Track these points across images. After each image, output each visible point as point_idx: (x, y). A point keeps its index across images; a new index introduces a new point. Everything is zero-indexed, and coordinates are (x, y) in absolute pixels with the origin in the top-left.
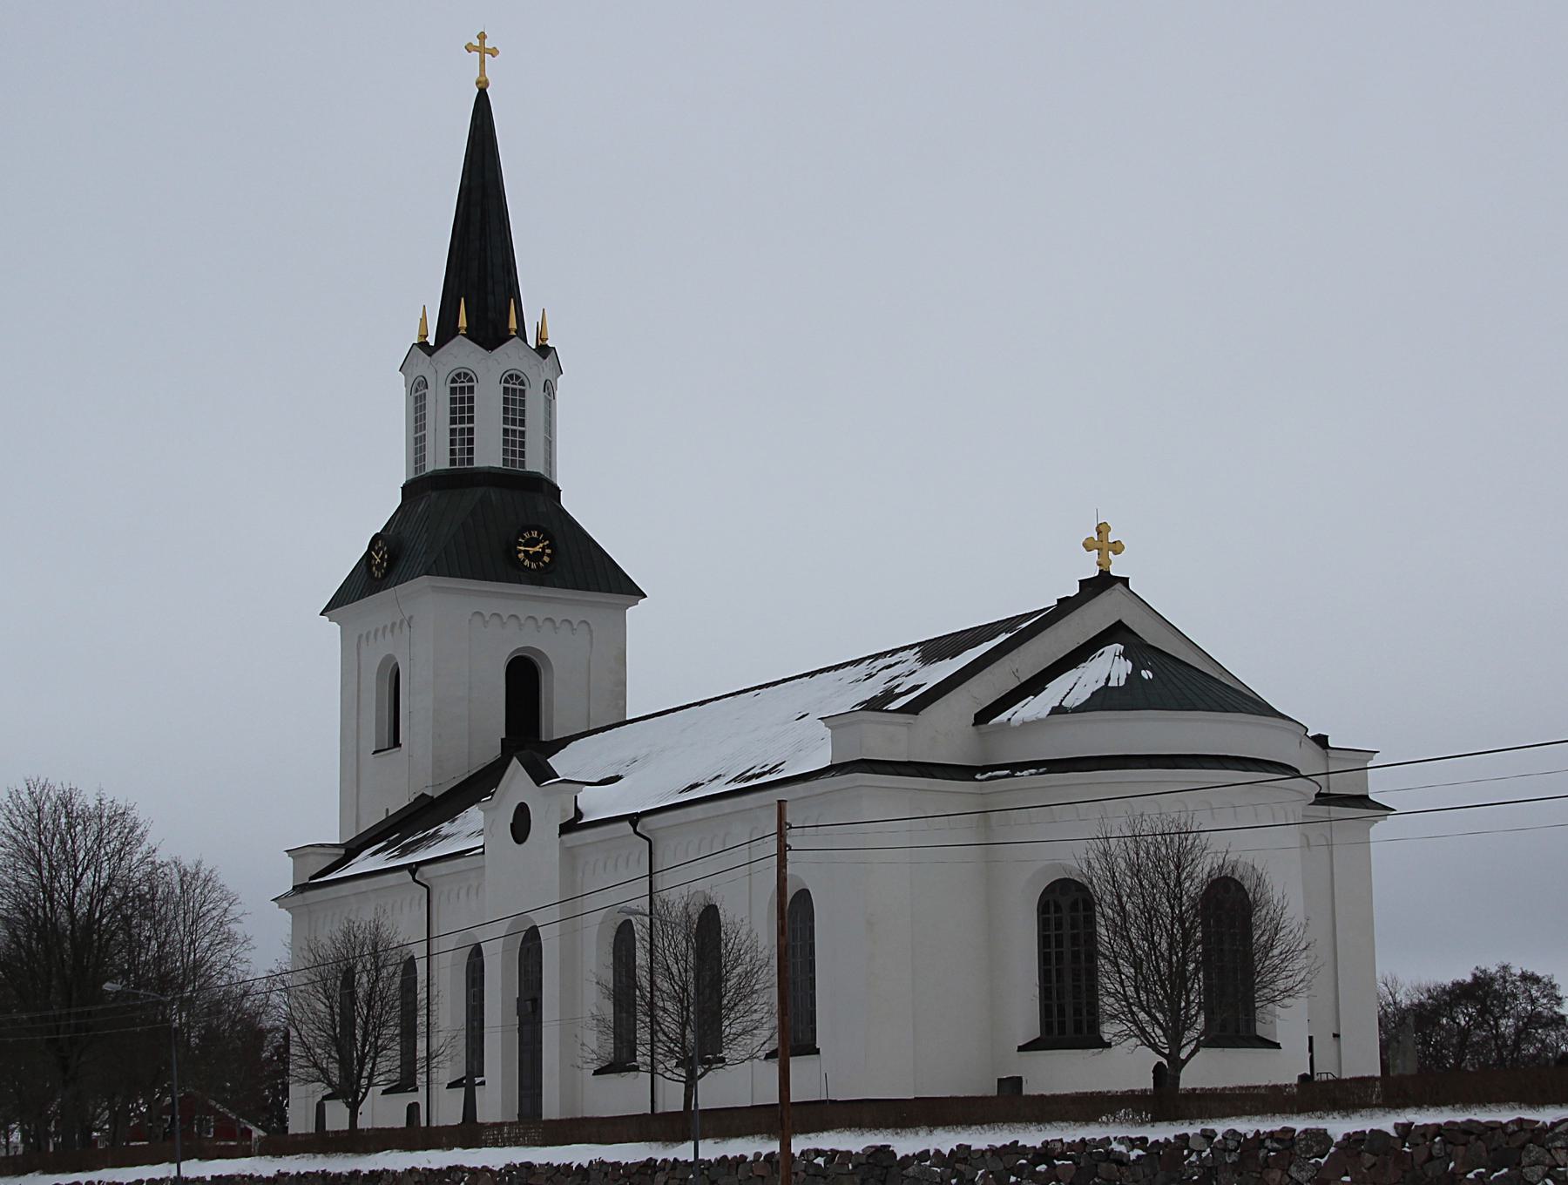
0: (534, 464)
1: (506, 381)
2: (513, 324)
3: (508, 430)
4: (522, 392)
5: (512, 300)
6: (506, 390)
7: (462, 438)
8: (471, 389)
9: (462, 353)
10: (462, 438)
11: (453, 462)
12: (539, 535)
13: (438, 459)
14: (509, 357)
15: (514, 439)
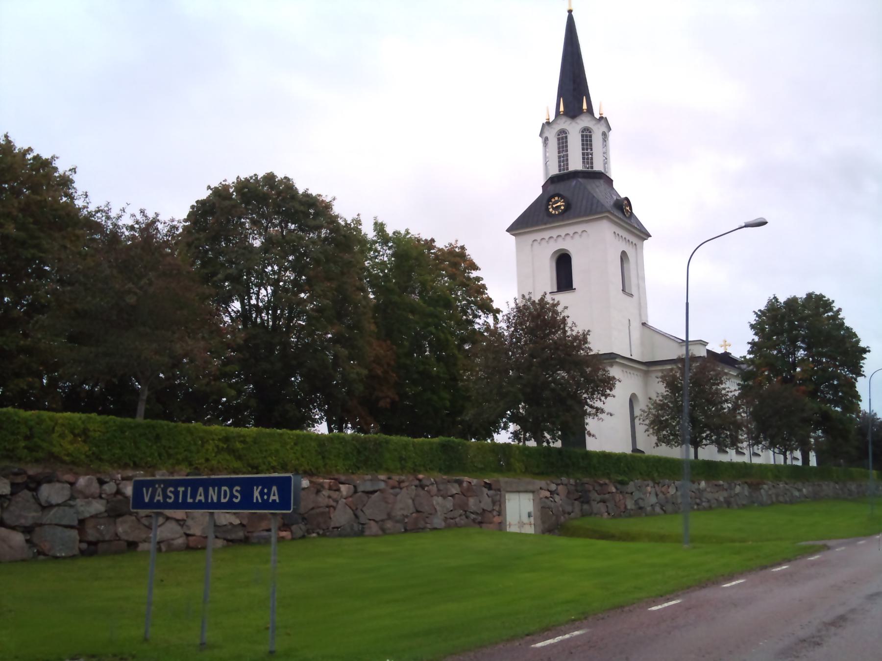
0: (598, 167)
1: (582, 132)
2: (585, 107)
3: (584, 153)
4: (591, 136)
5: (584, 98)
6: (582, 136)
7: (563, 159)
8: (566, 137)
9: (565, 124)
10: (563, 159)
11: (560, 170)
12: (558, 198)
13: (554, 171)
14: (584, 122)
15: (587, 157)
